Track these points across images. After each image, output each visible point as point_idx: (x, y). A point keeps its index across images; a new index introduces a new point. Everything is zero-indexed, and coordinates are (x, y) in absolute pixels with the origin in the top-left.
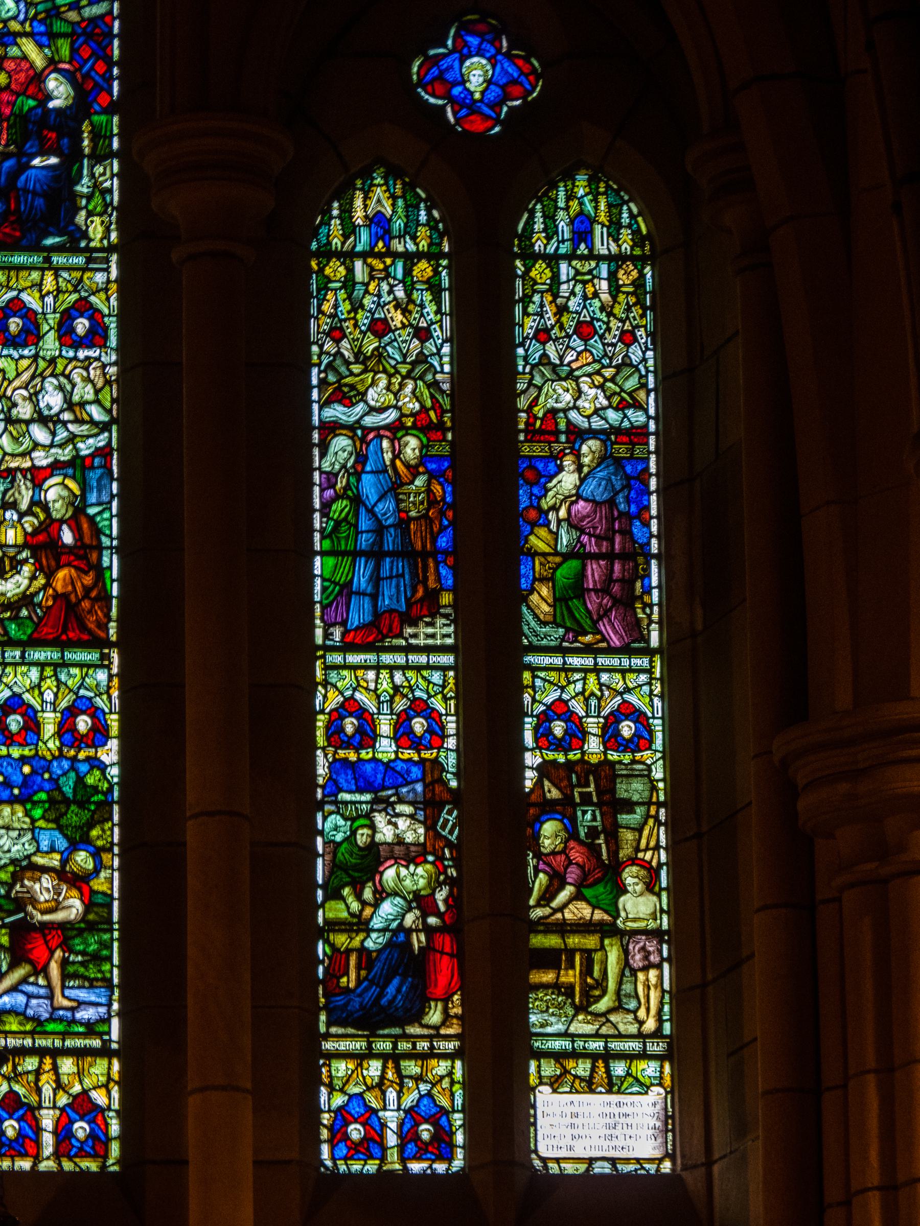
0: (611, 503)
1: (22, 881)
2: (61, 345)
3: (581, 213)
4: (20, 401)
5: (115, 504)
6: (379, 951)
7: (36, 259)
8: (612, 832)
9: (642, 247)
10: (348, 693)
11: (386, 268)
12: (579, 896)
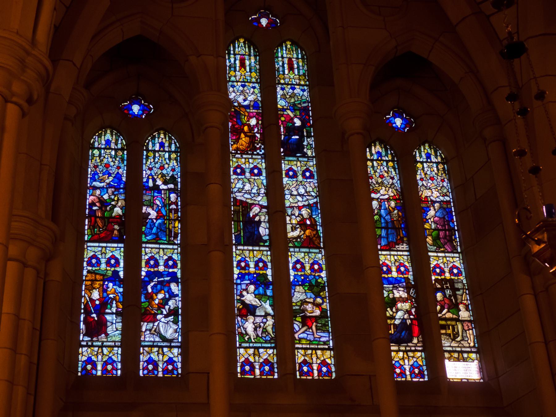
0: (444, 218)
1: (303, 305)
2: (303, 178)
3: (428, 153)
4: (294, 191)
5: (320, 215)
6: (399, 324)
7: (295, 159)
8: (455, 296)
9: (444, 160)
10: (383, 261)
11: (382, 163)
12: (448, 312)
